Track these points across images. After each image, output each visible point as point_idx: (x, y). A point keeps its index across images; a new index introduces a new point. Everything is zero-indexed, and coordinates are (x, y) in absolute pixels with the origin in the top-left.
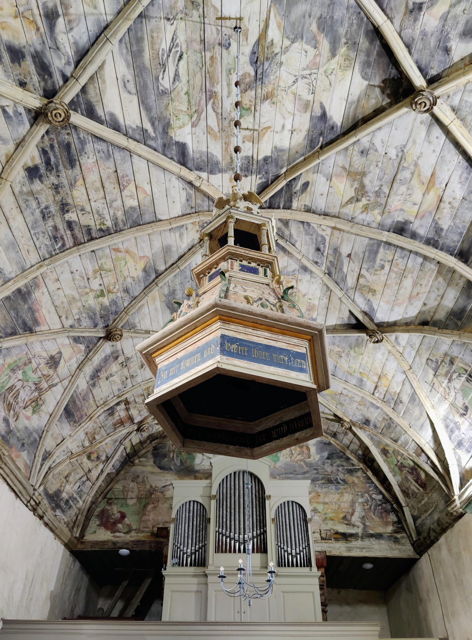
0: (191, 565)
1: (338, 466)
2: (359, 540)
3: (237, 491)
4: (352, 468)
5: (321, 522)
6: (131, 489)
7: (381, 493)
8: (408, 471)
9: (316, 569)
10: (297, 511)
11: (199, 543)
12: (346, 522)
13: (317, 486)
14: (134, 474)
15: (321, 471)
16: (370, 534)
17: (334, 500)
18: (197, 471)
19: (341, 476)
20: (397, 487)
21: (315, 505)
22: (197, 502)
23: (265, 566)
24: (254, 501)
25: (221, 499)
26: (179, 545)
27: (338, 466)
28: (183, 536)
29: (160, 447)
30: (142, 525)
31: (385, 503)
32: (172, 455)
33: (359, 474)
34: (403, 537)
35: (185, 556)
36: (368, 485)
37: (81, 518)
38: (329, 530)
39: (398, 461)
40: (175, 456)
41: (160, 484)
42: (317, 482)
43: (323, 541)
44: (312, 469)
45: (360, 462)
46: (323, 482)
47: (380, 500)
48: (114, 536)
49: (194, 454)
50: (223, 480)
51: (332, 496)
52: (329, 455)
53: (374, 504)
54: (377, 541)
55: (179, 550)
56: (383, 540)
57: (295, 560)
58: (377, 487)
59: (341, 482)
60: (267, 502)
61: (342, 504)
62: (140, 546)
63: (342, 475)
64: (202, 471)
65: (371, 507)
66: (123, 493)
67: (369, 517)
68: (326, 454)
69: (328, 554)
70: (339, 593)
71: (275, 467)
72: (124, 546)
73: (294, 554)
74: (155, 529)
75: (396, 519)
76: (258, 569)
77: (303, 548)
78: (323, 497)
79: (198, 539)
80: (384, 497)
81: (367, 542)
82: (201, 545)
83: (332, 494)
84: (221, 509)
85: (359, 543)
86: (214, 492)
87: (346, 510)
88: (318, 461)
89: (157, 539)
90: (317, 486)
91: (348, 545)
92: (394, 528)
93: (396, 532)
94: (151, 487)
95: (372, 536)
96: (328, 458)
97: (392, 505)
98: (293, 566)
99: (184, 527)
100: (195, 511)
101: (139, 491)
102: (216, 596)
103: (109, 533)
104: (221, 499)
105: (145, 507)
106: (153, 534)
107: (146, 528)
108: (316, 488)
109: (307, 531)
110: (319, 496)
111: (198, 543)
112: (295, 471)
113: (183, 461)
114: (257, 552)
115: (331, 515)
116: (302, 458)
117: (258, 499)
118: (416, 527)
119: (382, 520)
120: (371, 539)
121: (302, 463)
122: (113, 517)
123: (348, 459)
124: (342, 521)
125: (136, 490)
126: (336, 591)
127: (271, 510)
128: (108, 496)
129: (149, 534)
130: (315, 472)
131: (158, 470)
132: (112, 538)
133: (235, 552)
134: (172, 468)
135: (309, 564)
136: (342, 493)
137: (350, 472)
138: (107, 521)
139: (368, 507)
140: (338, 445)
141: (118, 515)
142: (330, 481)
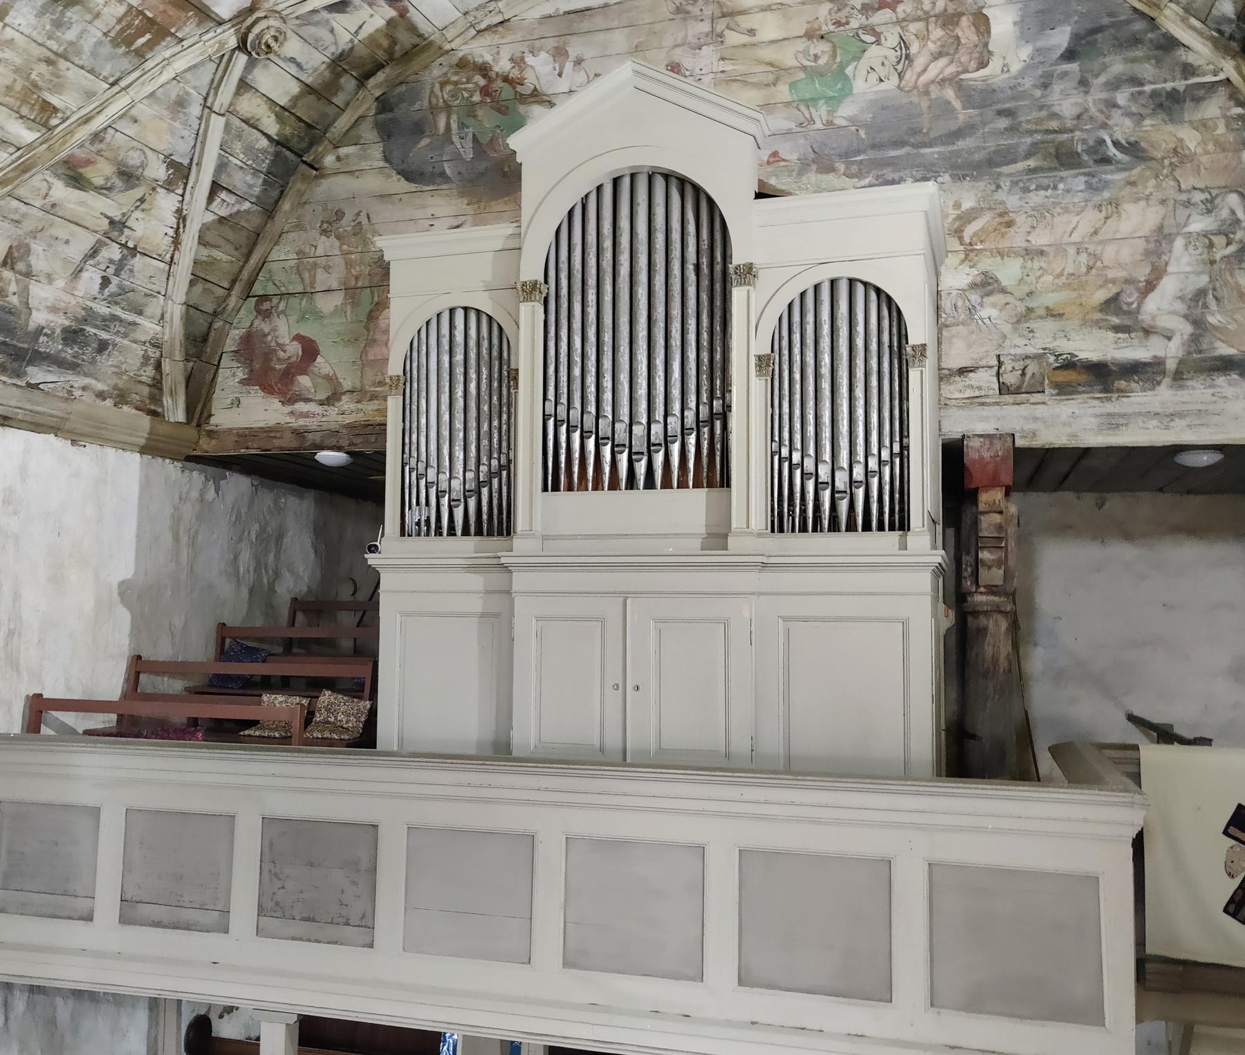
0: (466, 532)
1: (1115, 85)
3: (624, 259)
4: (1180, 85)
5: (1007, 328)
6: (322, 261)
10: (868, 314)
11: (490, 458)
12: (1115, 320)
13: (1005, 183)
15: (1028, 117)
16: (1216, 358)
17: (1076, 237)
19: (1123, 128)
21: (987, 263)
22: (478, 312)
23: (718, 537)
24: (691, 291)
25: (564, 292)
26: (421, 466)
27: (1115, 84)
30: (370, 376)
35: (445, 501)
37: (174, 371)
38: (1038, 357)
40: (454, 126)
42: (1005, 169)
43: (1008, 398)
44: (990, 113)
45: (1226, 51)
46: (1032, 163)
48: (292, 413)
49: (522, 109)
50: (571, 213)
51: (1063, 223)
52: (1076, 37)
55: (423, 482)
57: (843, 506)
60: (738, 295)
61: (1109, 253)
63: (1128, 122)
66: (299, 273)
68: (1061, 38)
69: (1020, 443)
70: (1100, 505)
71: (830, 123)
72: (327, 442)
76: (697, 543)
77: (880, 463)
79: (485, 442)
81: (1198, 392)
83: (1066, 210)
85: (1164, 396)
86: (532, 270)
87: (1122, 274)
88: (1022, 73)
90: (1005, 183)
91: (1110, 407)
98: (834, 526)
99: (433, 405)
100: (472, 343)
101: (349, 264)
103: (275, 403)
104: (564, 292)
108: (1001, 196)
109: (904, 396)
110: (1009, 224)
112: (915, 132)
113: (484, 140)
114: (697, 485)
115: (1051, 299)
116: (951, 69)
117: (705, 283)
121: (949, 93)
122: (281, 354)
123: (1170, 44)
124: (1098, 316)
125: (338, 261)
126: (1089, 499)
128: (258, 289)
130: (1003, 123)
131: (403, 185)
132: (288, 419)
134: (448, 171)
136: (1115, 203)
138: (267, 369)
141: (295, 349)
142: (1065, 158)
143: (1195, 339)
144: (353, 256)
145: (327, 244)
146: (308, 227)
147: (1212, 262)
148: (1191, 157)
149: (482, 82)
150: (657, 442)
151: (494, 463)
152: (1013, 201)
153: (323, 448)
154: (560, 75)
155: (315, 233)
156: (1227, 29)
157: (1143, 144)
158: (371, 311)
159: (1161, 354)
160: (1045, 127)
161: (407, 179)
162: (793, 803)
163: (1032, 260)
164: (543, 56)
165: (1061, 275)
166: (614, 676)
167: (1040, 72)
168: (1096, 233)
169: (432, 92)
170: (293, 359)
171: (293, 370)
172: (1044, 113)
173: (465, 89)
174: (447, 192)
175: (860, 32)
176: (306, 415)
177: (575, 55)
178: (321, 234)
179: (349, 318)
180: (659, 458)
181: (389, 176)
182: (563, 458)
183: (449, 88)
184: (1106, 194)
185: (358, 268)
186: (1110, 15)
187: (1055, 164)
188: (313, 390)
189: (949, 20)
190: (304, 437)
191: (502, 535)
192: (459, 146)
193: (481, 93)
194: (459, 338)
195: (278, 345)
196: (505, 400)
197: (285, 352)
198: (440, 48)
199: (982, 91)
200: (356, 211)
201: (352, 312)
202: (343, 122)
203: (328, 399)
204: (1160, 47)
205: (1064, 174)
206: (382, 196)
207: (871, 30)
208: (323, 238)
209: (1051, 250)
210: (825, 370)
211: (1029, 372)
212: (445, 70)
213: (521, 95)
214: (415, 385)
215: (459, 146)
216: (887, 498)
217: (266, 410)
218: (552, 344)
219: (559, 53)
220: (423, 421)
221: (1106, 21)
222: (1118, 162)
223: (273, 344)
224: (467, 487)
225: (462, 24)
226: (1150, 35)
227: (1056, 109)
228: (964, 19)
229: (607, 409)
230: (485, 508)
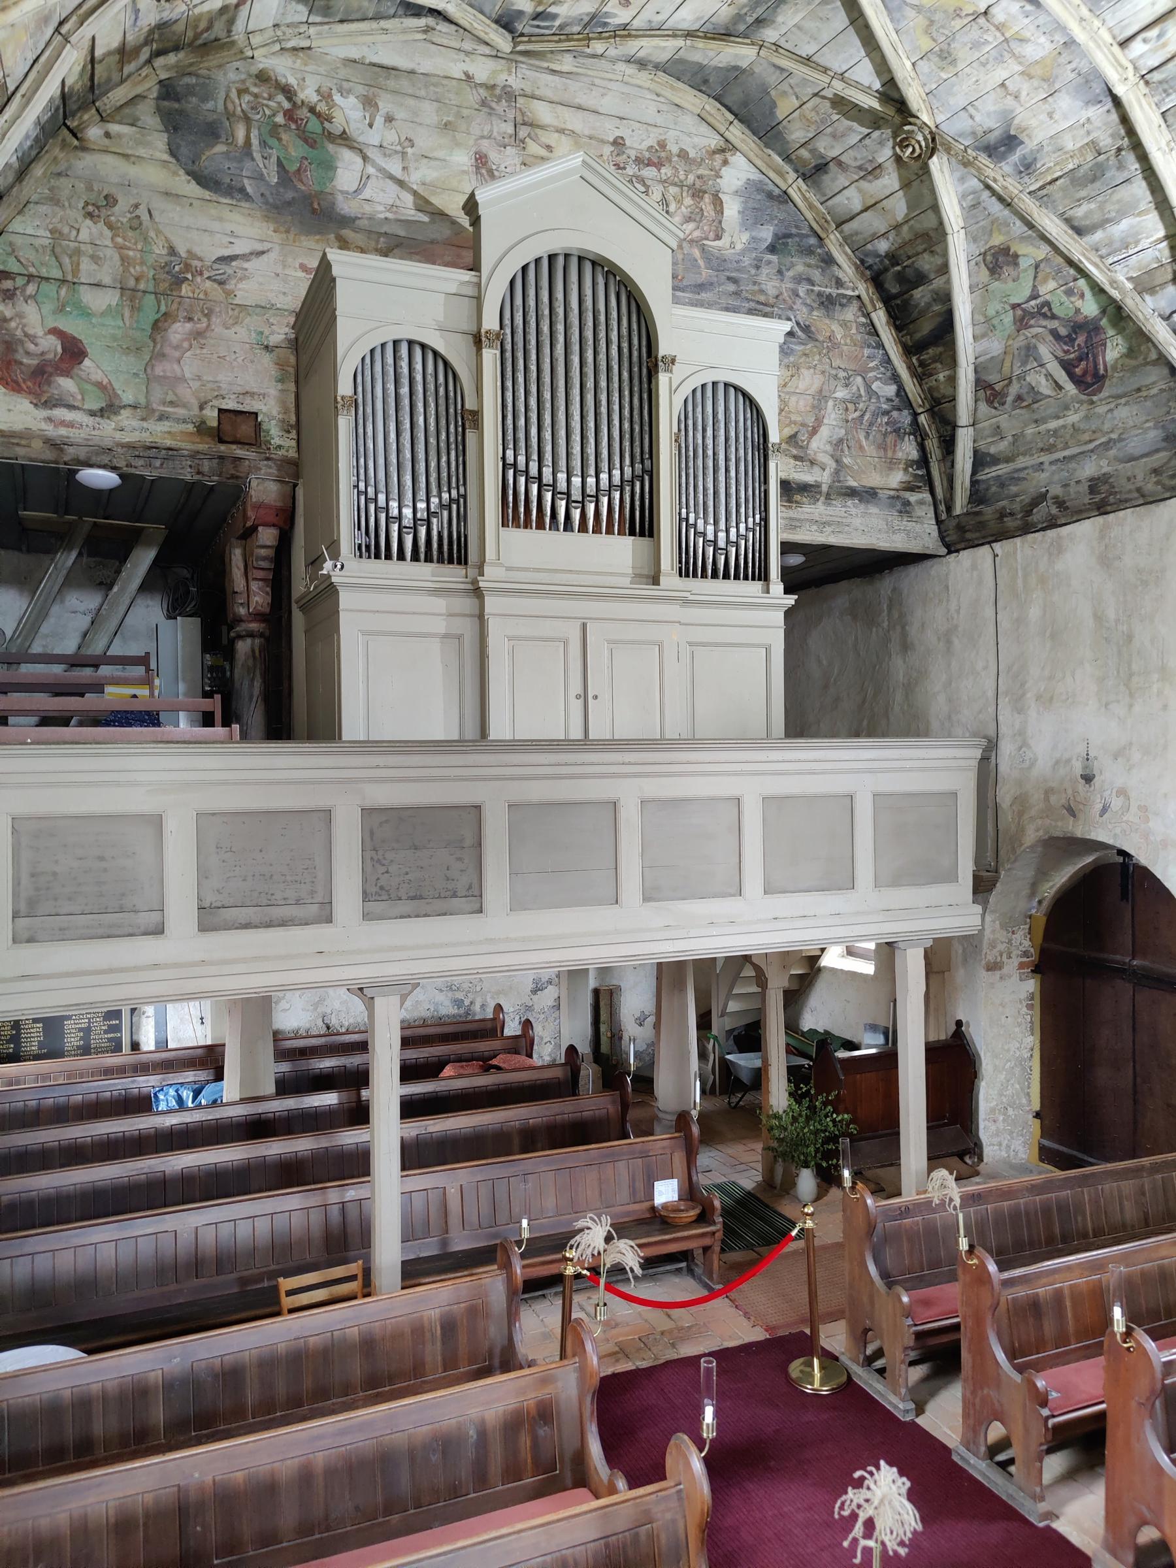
0: (415, 558)
1: (799, 279)
2: (820, 503)
3: (560, 328)
4: (834, 292)
7: (896, 378)
8: (1054, 333)
9: (781, 587)
12: (795, 452)
14: (90, 188)
16: (848, 488)
18: (346, 221)
20: (971, 369)
22: (424, 347)
26: (371, 490)
27: (799, 279)
28: (381, 461)
31: (899, 410)
32: (240, 134)
33: (851, 313)
34: (921, 502)
35: (395, 527)
36: (867, 352)
39: (1034, 296)
40: (255, 142)
41: (210, 249)
47: (889, 400)
48: (50, 419)
49: (331, 147)
52: (777, 237)
53: (872, 408)
54: (862, 507)
55: (372, 507)
56: (876, 505)
58: (889, 361)
59: (800, 333)
60: (663, 378)
62: (158, 463)
63: (805, 310)
64: (363, 223)
65: (862, 416)
67: (852, 443)
68: (767, 234)
74: (211, 416)
75: (914, 454)
76: (626, 581)
80: (901, 390)
81: (836, 509)
86: (490, 322)
87: (799, 419)
88: (743, 252)
89: (223, 447)
92: (907, 478)
93: (910, 488)
94: (172, 251)
95: (852, 493)
96: (772, 249)
97: (915, 415)
98: (715, 575)
99: (382, 430)
100: (419, 377)
105: (157, 327)
106: (202, 429)
107: (171, 403)
111: (434, 491)
116: (697, 234)
118: (974, 483)
119: (882, 453)
120: (849, 503)
121: (697, 253)
122: (31, 347)
123: (828, 261)
129: (190, 428)
130: (732, 288)
131: (192, 189)
132: (44, 426)
134: (249, 190)
135: (763, 575)
137: (828, 303)
139: (857, 414)
140: (811, 207)
141: (52, 346)
143: (837, 472)
144: (131, 253)
145: (94, 230)
146: (66, 204)
147: (847, 421)
148: (836, 345)
149: (287, 105)
153: (91, 466)
154: (371, 125)
155: (75, 214)
156: (870, 261)
157: (813, 329)
158: (156, 322)
159: (819, 479)
161: (198, 184)
162: (799, 761)
164: (352, 100)
166: (576, 687)
168: (785, 386)
169: (227, 96)
170: (50, 356)
171: (50, 369)
172: (756, 288)
173: (267, 106)
174: (246, 211)
176: (63, 423)
177: (386, 110)
178: (85, 217)
179: (128, 324)
180: (591, 508)
181: (175, 173)
182: (511, 498)
183: (247, 98)
184: (792, 359)
185: (138, 268)
186: (797, 227)
188: (79, 397)
189: (697, 194)
190: (62, 450)
191: (443, 562)
192: (261, 165)
193: (285, 115)
195: (26, 335)
197: (36, 345)
198: (242, 52)
200: (133, 201)
201: (131, 317)
202: (119, 95)
203: (102, 410)
204: (823, 261)
207: (642, 181)
208: (88, 222)
212: (243, 77)
213: (330, 133)
214: (452, 410)
215: (261, 165)
217: (9, 410)
219: (369, 103)
221: (794, 231)
222: (799, 337)
223: (19, 333)
224: (419, 515)
225: (270, 33)
226: (819, 250)
227: (763, 287)
228: (706, 195)
229: (562, 463)
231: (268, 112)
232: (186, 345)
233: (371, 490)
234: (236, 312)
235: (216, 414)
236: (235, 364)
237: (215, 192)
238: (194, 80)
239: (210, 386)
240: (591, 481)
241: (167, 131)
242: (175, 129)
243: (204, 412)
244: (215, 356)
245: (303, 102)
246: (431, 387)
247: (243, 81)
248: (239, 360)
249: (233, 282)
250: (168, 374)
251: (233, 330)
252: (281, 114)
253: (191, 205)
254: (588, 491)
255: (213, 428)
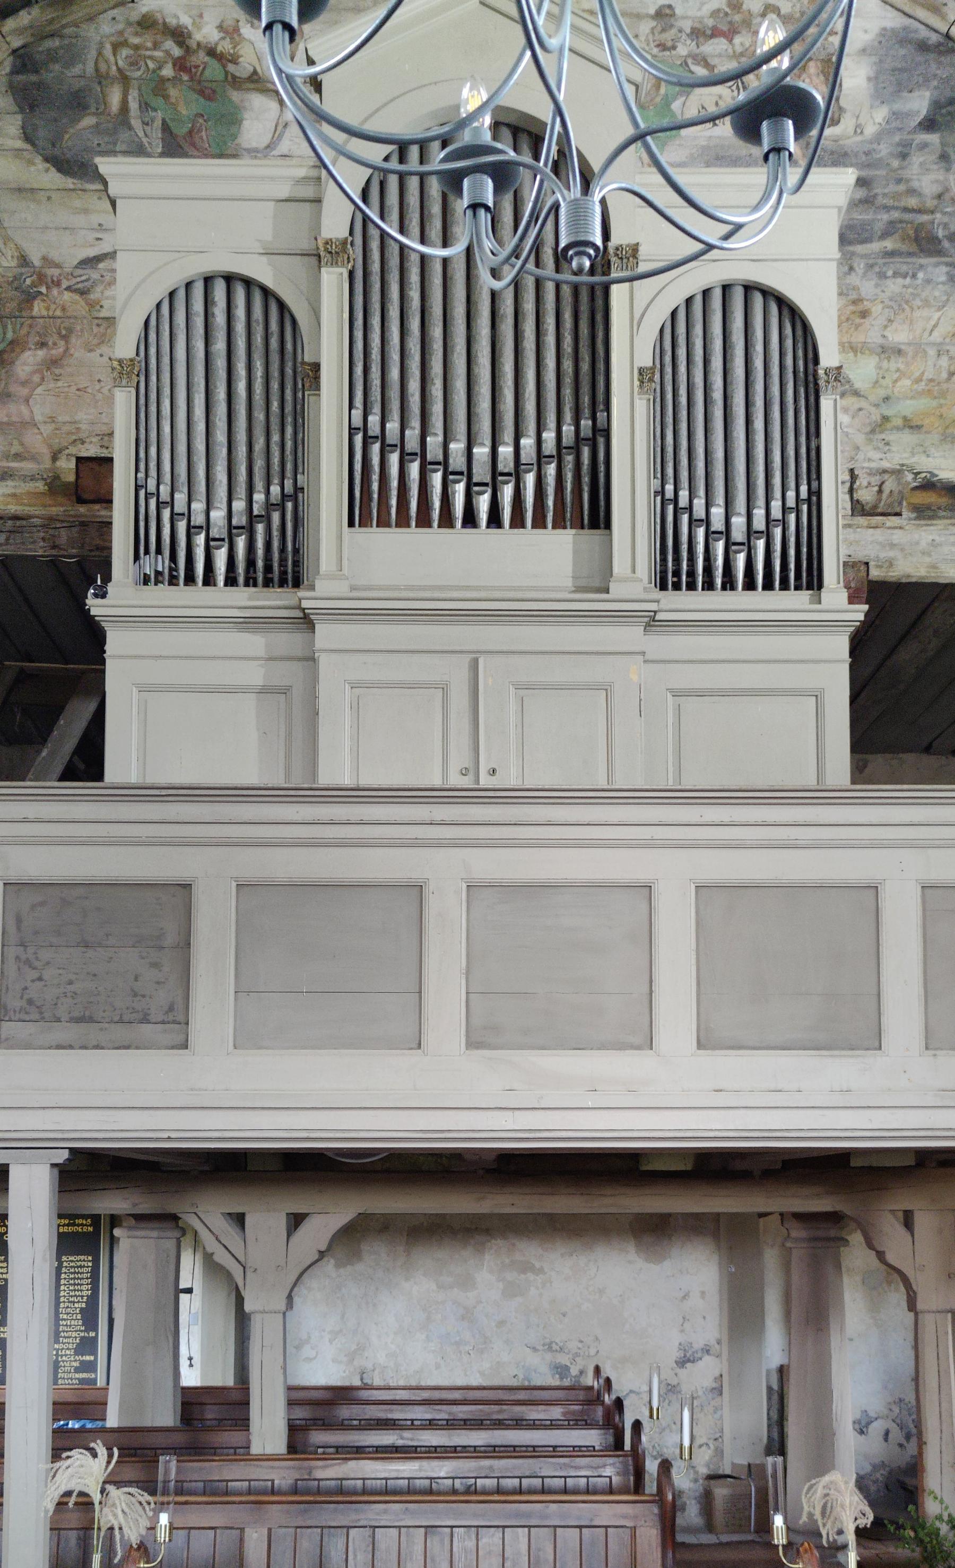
0: (231, 581)
13: (860, 266)
17: (937, 336)
22: (248, 283)
25: (376, 267)
26: (165, 490)
28: (182, 448)
29: (52, 57)
32: (115, 99)
35: (200, 540)
40: (133, 105)
42: (860, 249)
46: (889, 244)
55: (166, 514)
73: (738, 534)
74: (67, 466)
77: (785, 509)
78: (882, 321)
82: (275, 490)
83: (926, 304)
84: (376, 321)
88: (878, 138)
90: (860, 266)
94: (24, 261)
98: (729, 583)
102: (356, 707)
108: (854, 279)
109: (814, 430)
110: (864, 314)
111: (259, 484)
113: (181, 130)
114: (559, 524)
115: (908, 407)
127: (635, 324)
131: (51, 178)
133: (447, 520)
149: (177, 52)
150: (506, 470)
151: (275, 490)
152: (868, 288)
160: (903, 204)
161: (60, 170)
163: (889, 359)
165: (918, 380)
167: (897, 138)
169: (100, 54)
172: (902, 187)
173: (151, 57)
175: (690, 61)
181: (31, 163)
182: (375, 486)
183: (125, 52)
187: (914, 248)
192: (141, 134)
194: (220, 318)
196: (289, 408)
199: (832, 153)
205: (924, 261)
206: (20, 190)
209: (910, 351)
210: (717, 395)
211: (887, 488)
212: (120, 27)
215: (141, 134)
216: (792, 552)
218: (359, 334)
220: (167, 429)
224: (235, 522)
230: (260, 552)
231: (151, 65)
232: (36, 378)
233: (165, 490)
234: (102, 329)
235: (72, 464)
236: (99, 396)
237: (81, 178)
238: (57, 42)
239: (66, 428)
240: (506, 451)
241: (22, 110)
242: (32, 107)
243: (58, 464)
244: (73, 389)
245: (199, 44)
246: (258, 339)
247: (121, 33)
248: (105, 391)
249: (99, 289)
250: (14, 419)
251: (99, 351)
252: (170, 65)
253: (49, 198)
254: (501, 467)
255: (69, 483)
